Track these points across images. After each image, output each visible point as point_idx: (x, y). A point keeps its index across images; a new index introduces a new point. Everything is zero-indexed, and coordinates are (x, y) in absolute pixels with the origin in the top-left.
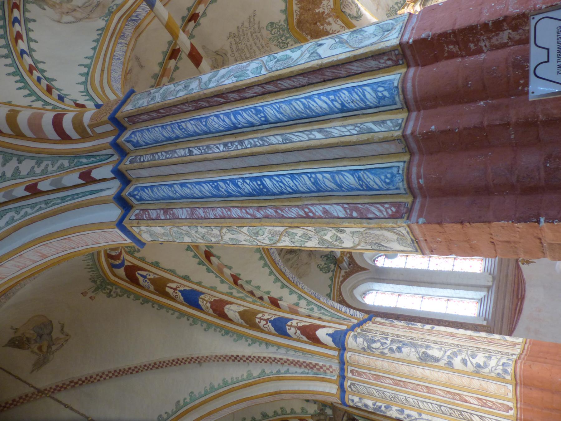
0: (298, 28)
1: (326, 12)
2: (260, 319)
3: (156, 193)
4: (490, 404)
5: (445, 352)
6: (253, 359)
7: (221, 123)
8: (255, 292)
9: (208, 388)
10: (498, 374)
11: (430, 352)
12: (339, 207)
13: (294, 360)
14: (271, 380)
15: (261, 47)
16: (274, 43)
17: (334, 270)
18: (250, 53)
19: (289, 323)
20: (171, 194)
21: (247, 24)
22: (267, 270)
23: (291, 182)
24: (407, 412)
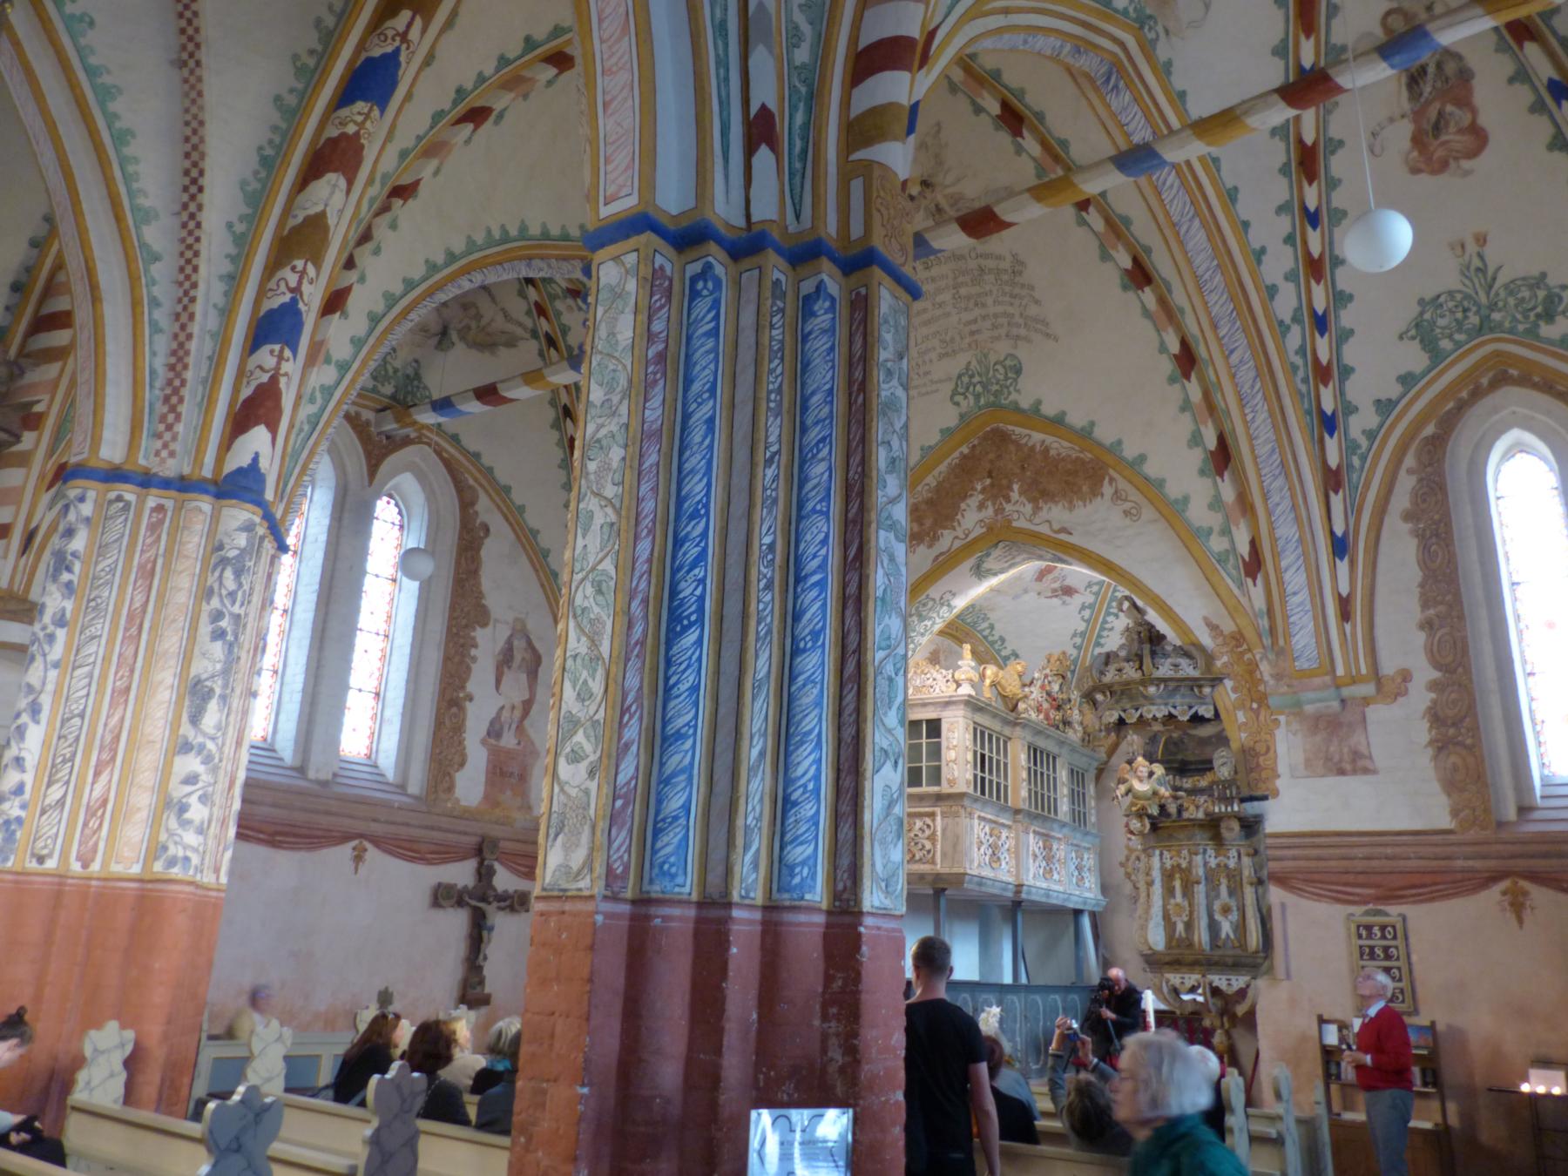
1: (1008, 507)
2: (303, 273)
3: (702, 345)
4: (93, 823)
5: (213, 739)
6: (190, 233)
7: (812, 550)
8: (369, 246)
9: (106, 79)
10: (165, 848)
11: (213, 705)
12: (632, 770)
13: (187, 353)
14: (133, 280)
15: (974, 328)
16: (974, 363)
17: (378, 392)
18: (968, 298)
19: (287, 353)
20: (696, 387)
21: (1033, 310)
22: (417, 272)
23: (687, 685)
24: (61, 634)
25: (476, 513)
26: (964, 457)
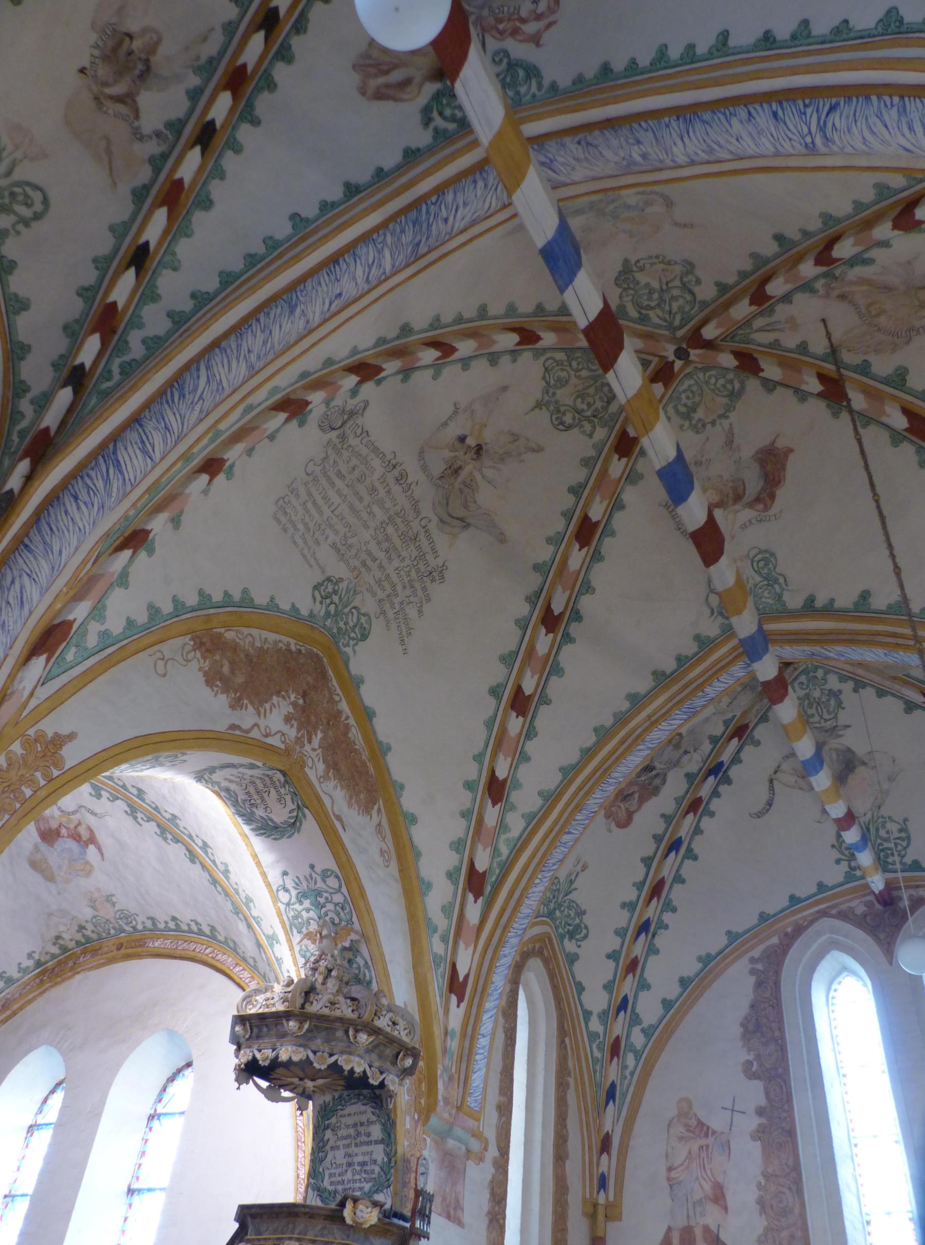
0: (317, 655)
18: (388, 539)
21: (412, 612)
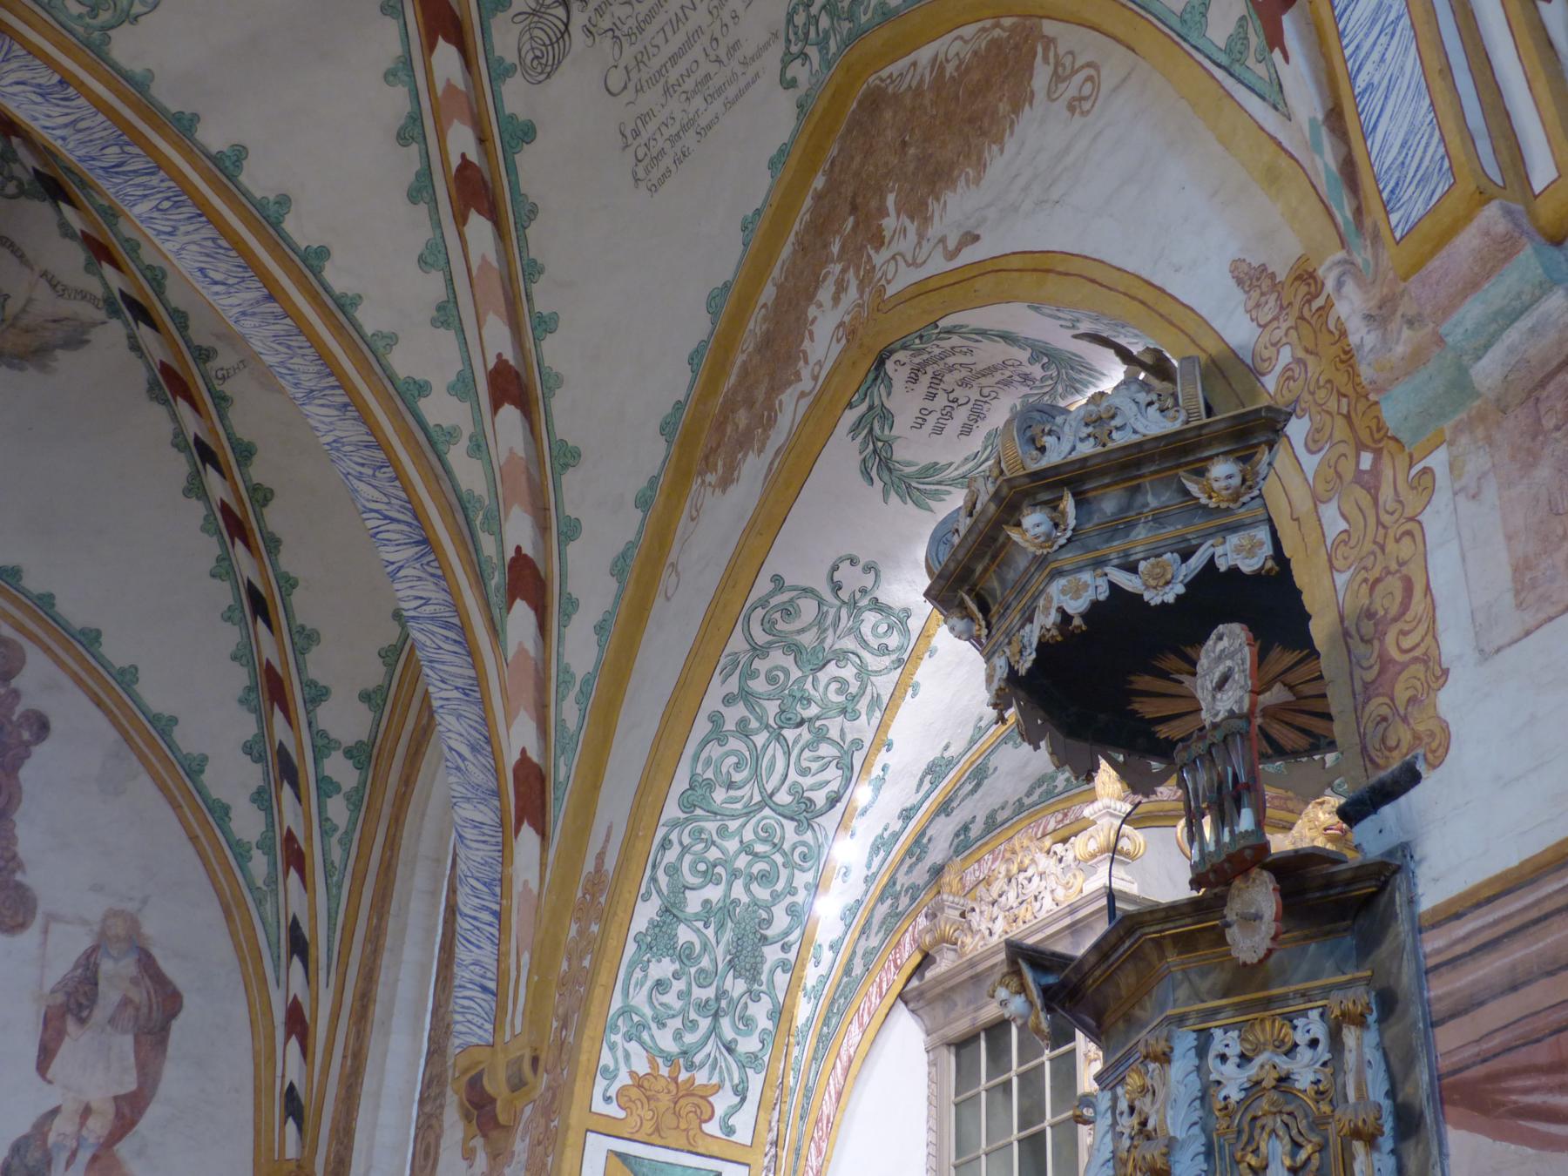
0: (860, 103)
25: (16, 694)
26: (819, 197)
